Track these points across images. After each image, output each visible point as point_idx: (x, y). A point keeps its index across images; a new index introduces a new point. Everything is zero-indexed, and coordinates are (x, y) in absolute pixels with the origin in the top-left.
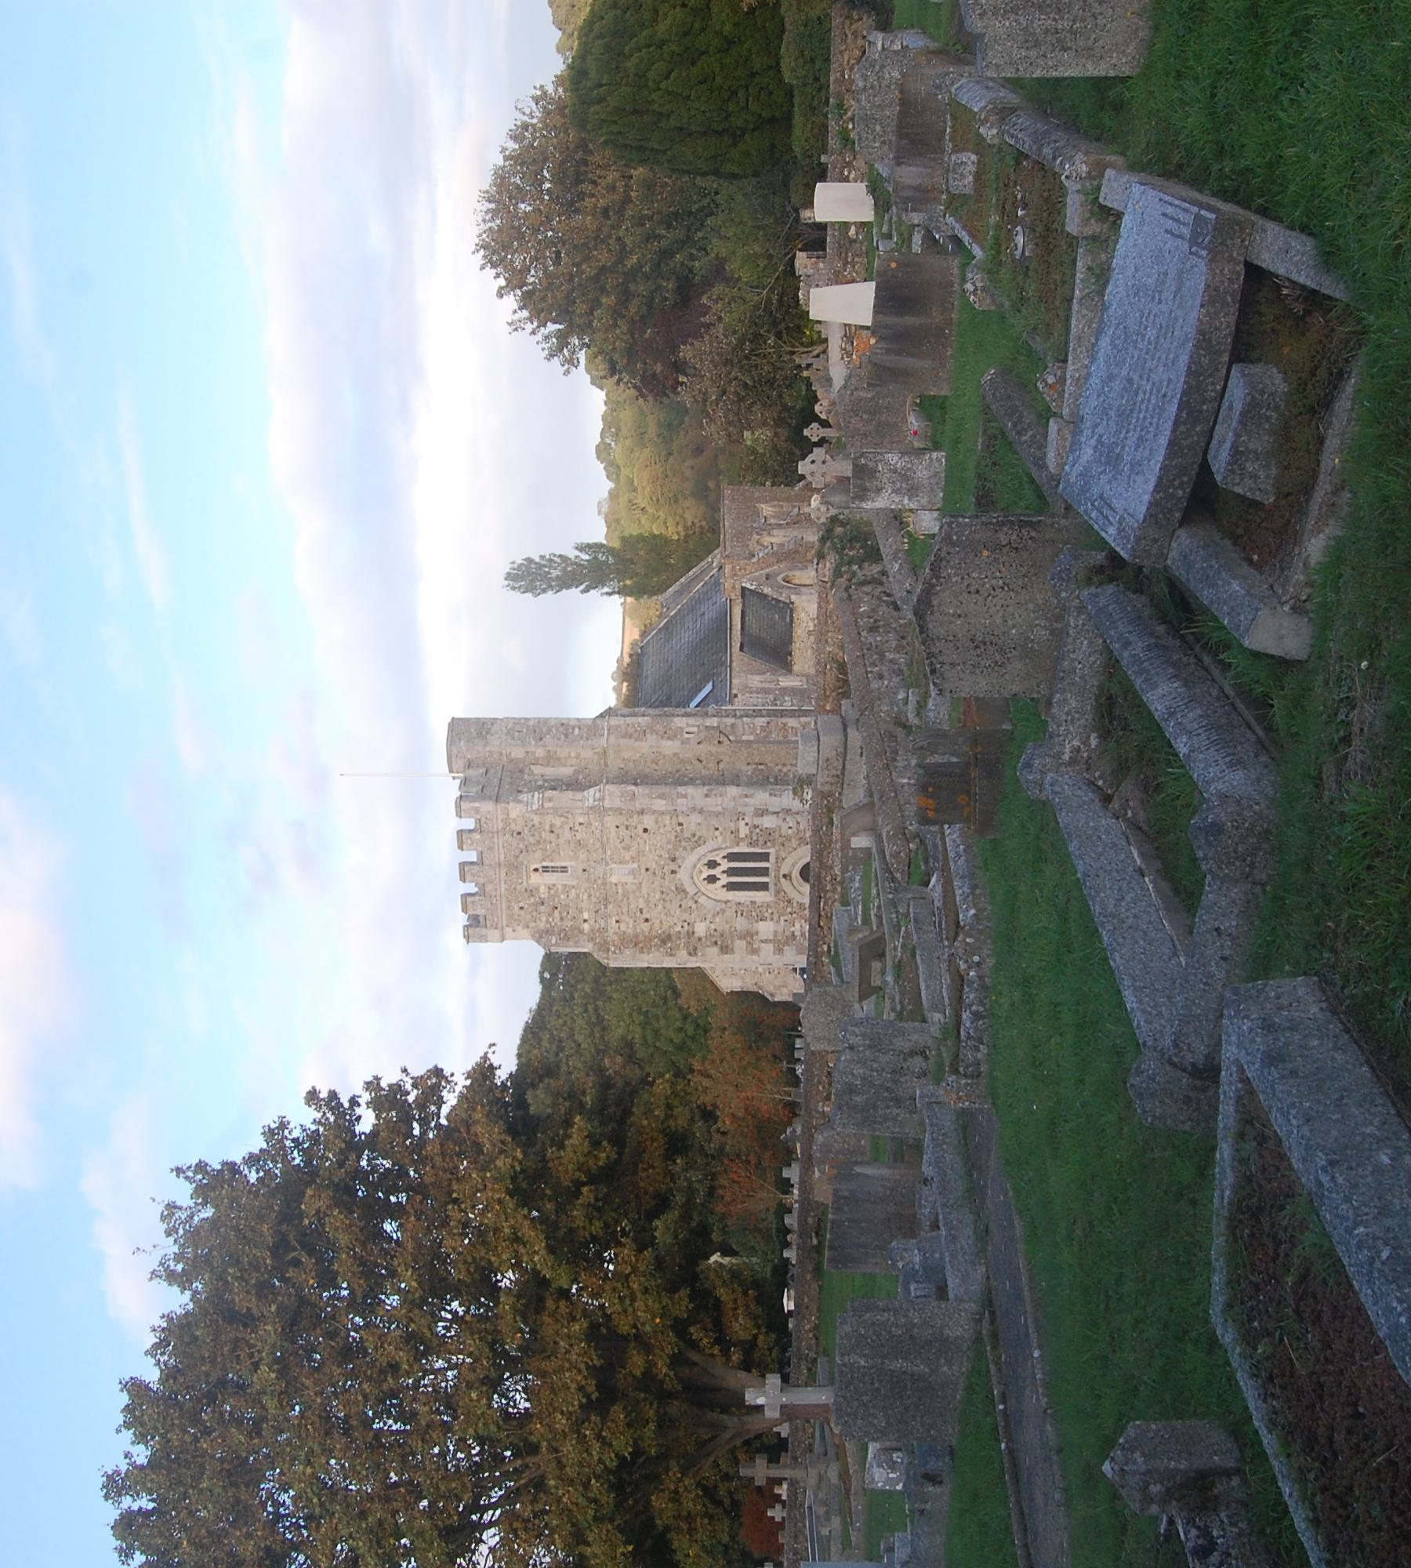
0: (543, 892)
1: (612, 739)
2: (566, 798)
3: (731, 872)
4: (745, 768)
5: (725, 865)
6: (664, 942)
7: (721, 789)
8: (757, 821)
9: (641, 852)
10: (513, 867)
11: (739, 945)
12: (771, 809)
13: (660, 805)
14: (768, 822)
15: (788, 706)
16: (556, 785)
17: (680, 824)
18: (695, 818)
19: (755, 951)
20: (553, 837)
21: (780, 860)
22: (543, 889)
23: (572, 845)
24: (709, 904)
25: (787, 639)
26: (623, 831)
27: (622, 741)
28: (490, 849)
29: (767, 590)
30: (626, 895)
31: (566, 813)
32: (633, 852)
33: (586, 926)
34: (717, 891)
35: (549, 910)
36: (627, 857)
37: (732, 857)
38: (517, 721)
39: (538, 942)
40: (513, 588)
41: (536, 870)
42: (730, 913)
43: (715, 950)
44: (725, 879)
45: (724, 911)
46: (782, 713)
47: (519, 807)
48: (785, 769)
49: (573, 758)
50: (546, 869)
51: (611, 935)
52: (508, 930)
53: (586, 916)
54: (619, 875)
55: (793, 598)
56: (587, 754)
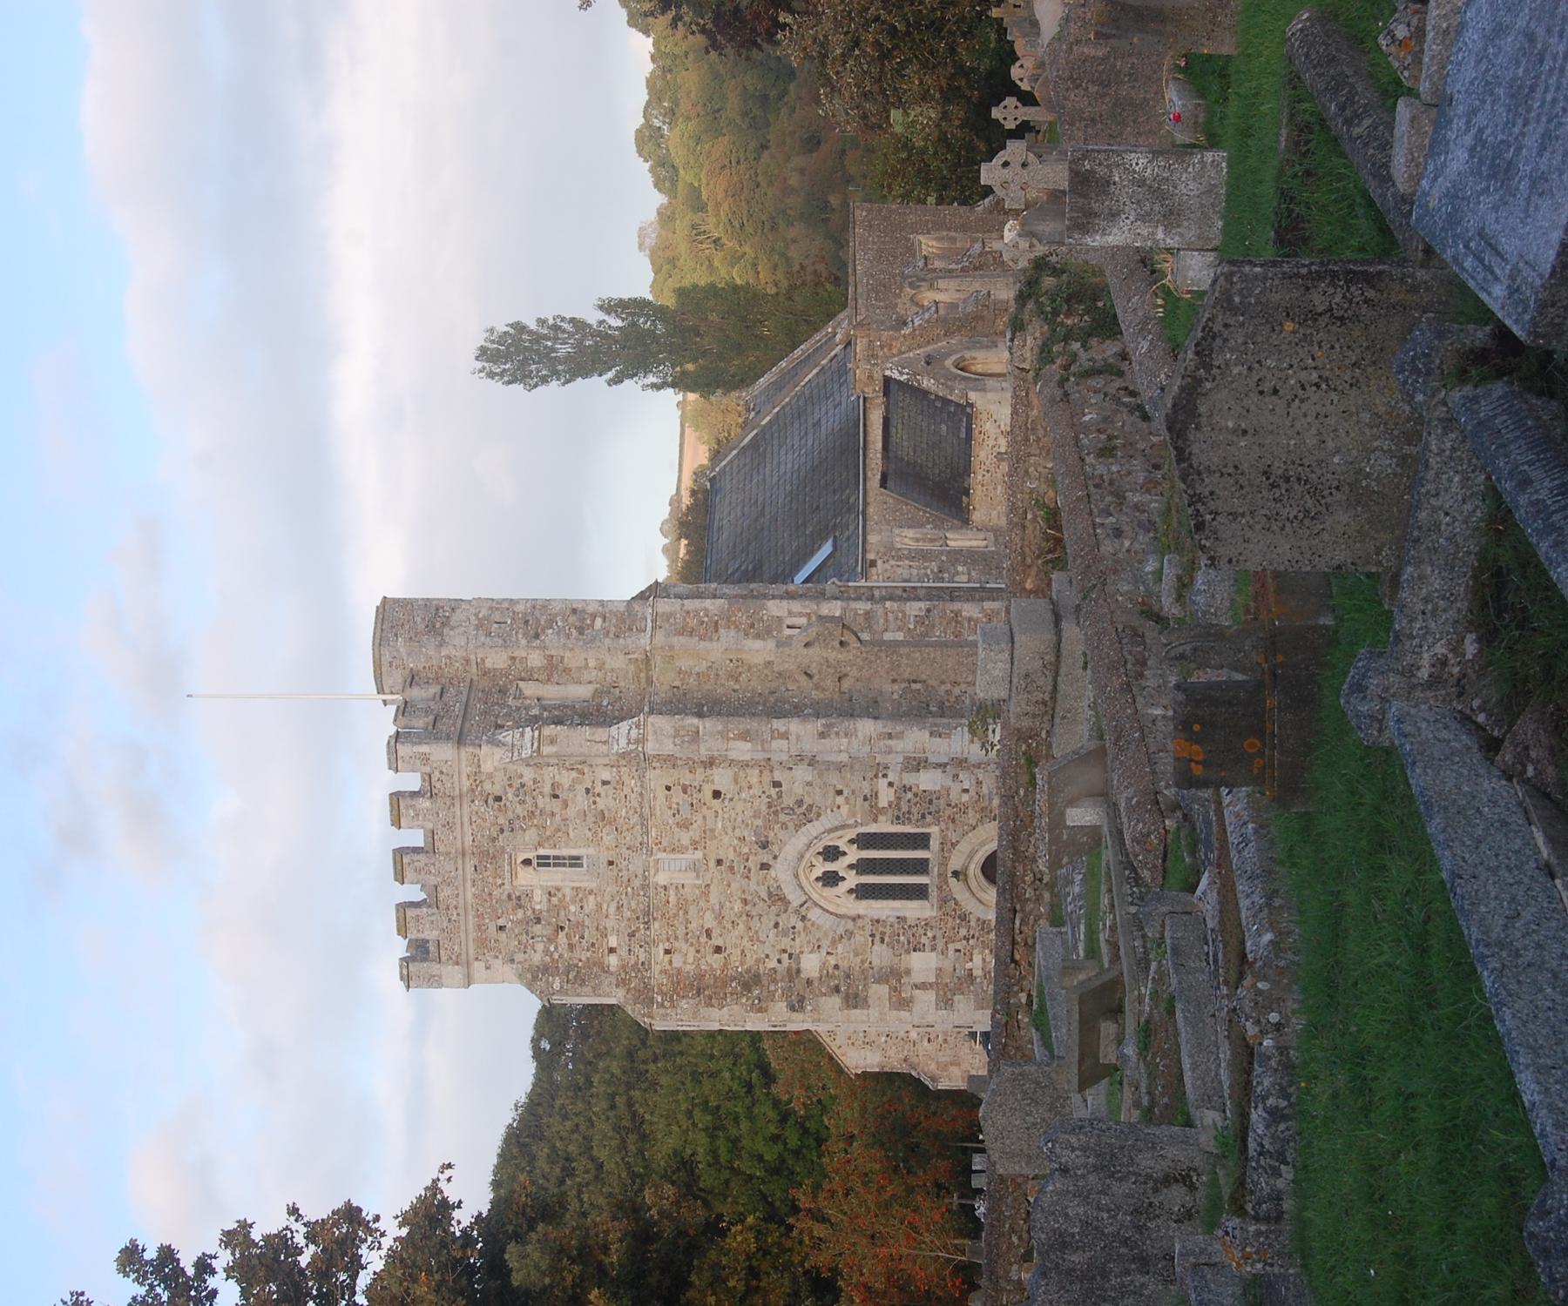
0: (539, 901)
1: (660, 638)
2: (578, 739)
3: (863, 867)
4: (888, 687)
5: (854, 855)
6: (747, 987)
7: (848, 724)
8: (909, 779)
9: (708, 834)
10: (488, 857)
11: (879, 992)
12: (933, 759)
13: (742, 750)
14: (927, 781)
15: (962, 581)
16: (563, 715)
17: (777, 784)
18: (803, 773)
19: (904, 1004)
20: (556, 805)
21: (948, 846)
22: (538, 896)
23: (590, 819)
24: (826, 922)
25: (962, 468)
26: (677, 796)
27: (678, 641)
28: (448, 825)
29: (927, 383)
30: (683, 906)
31: (579, 765)
33: (613, 960)
34: (840, 900)
35: (548, 931)
36: (686, 841)
37: (865, 841)
38: (495, 605)
39: (530, 986)
40: (491, 375)
41: (527, 862)
42: (861, 938)
43: (836, 1000)
44: (852, 880)
46: (952, 595)
47: (499, 753)
48: (957, 691)
49: (592, 668)
50: (544, 861)
51: (657, 977)
52: (478, 967)
54: (670, 871)
55: (973, 396)
56: (617, 662)
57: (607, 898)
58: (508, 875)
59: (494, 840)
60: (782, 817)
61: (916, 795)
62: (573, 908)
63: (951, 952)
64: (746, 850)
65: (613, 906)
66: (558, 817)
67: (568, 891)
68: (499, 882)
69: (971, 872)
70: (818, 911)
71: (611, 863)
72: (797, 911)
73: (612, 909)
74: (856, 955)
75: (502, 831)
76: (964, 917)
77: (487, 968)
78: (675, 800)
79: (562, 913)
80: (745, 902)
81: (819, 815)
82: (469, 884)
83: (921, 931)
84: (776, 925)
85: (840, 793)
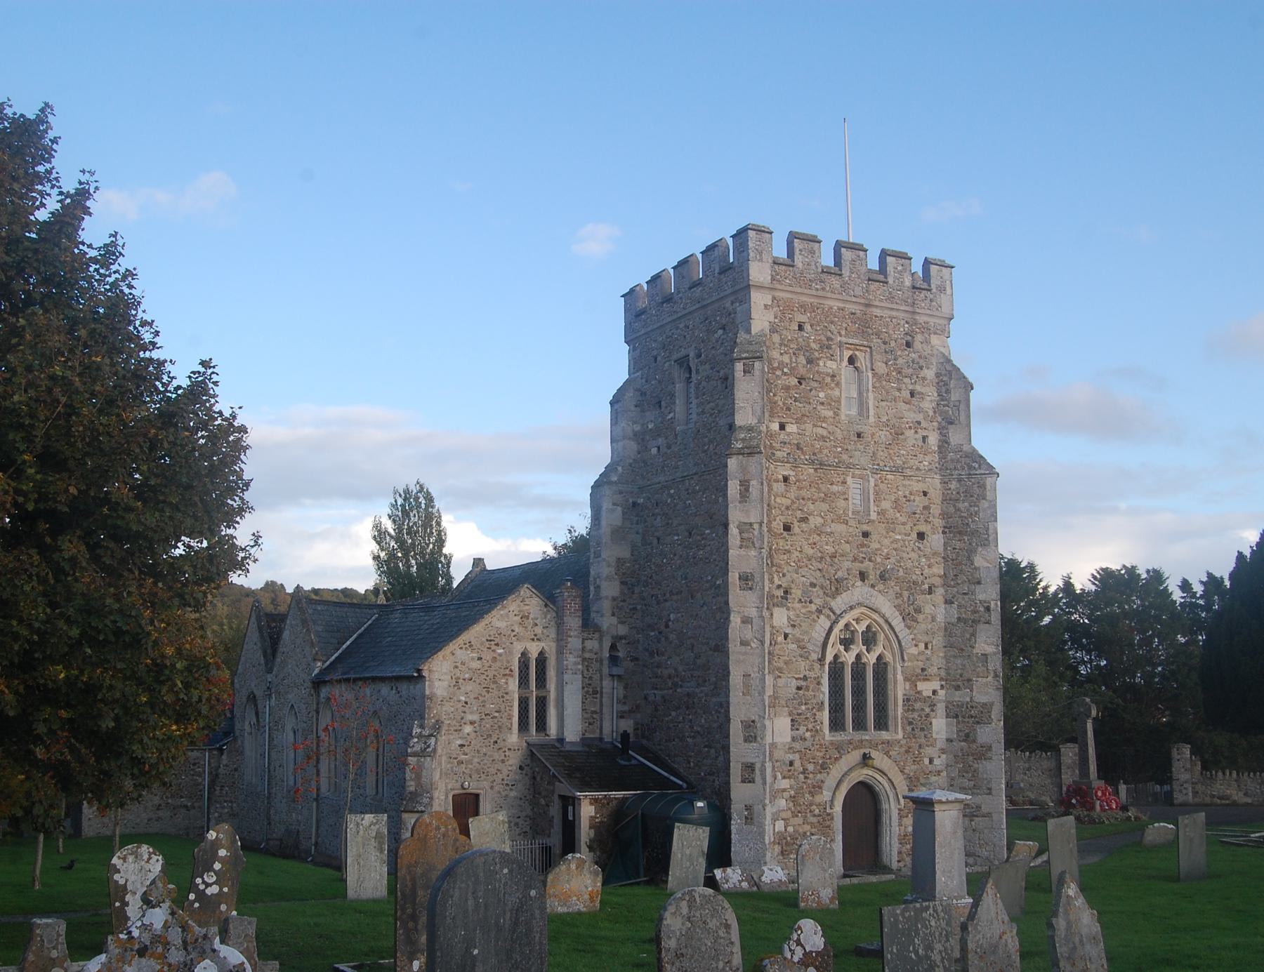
5: (871, 659)
9: (891, 525)
17: (930, 591)
26: (920, 501)
32: (891, 513)
35: (802, 371)
36: (886, 505)
37: (881, 668)
44: (849, 658)
45: (805, 657)
53: (791, 428)
57: (831, 428)
58: (850, 341)
59: (878, 335)
60: (906, 594)
61: (927, 716)
62: (822, 395)
63: (791, 757)
64: (879, 560)
65: (825, 433)
66: (897, 394)
67: (837, 393)
68: (843, 332)
69: (866, 771)
70: (828, 624)
71: (859, 435)
72: (826, 605)
73: (820, 431)
74: (786, 663)
75: (885, 343)
76: (824, 767)
77: (766, 306)
78: (917, 499)
79: (816, 385)
80: (833, 556)
81: (909, 628)
82: (841, 305)
83: (810, 726)
84: (813, 585)
85: (926, 647)
